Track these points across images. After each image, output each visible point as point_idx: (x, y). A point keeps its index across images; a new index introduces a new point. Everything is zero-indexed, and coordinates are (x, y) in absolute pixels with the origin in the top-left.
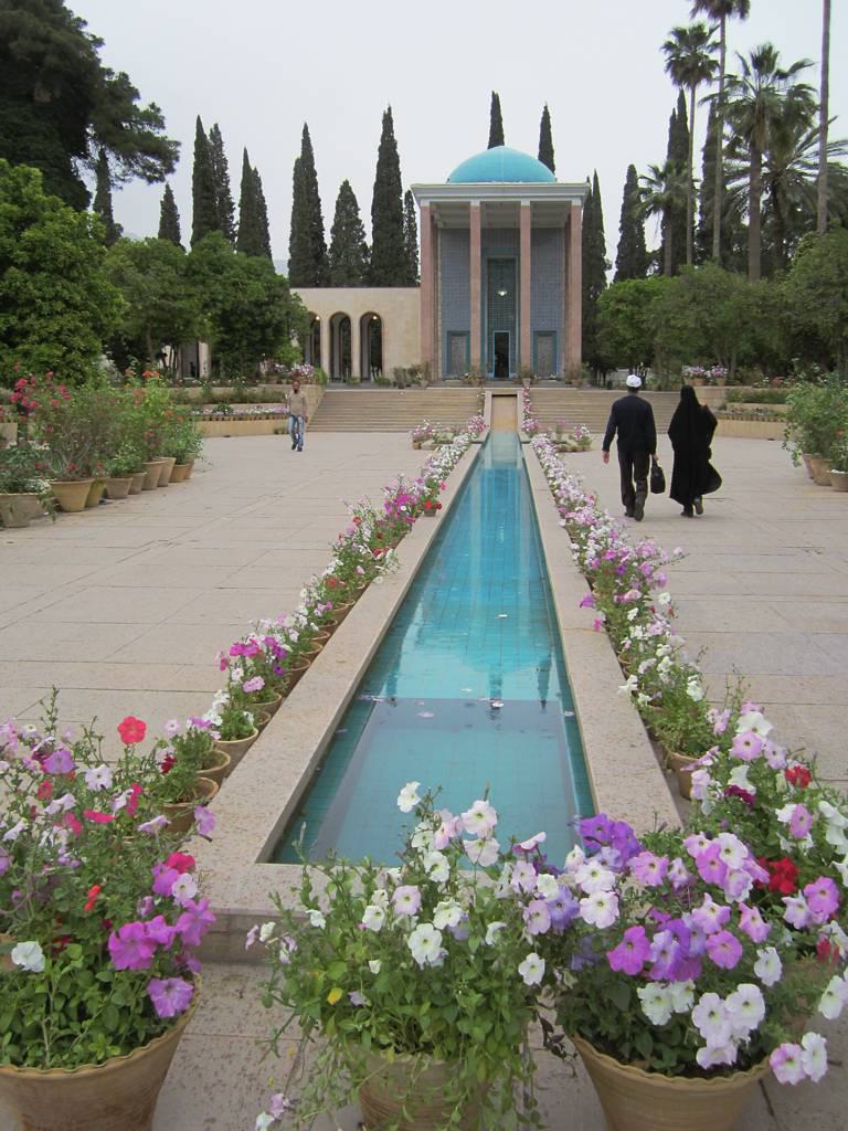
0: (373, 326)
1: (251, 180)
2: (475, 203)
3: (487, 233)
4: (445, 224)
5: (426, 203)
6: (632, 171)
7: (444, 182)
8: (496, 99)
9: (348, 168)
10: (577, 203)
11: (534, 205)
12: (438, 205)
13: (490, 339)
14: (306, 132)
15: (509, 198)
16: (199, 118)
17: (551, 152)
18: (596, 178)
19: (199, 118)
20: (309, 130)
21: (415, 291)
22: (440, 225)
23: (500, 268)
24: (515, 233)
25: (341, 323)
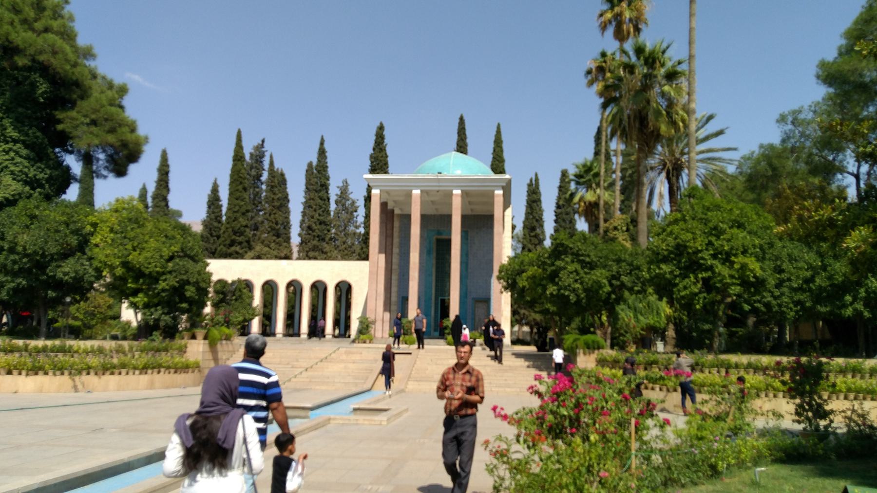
0: (344, 290)
1: (279, 181)
4: (401, 209)
6: (564, 174)
8: (462, 119)
9: (349, 174)
12: (388, 192)
13: (436, 304)
14: (322, 143)
18: (537, 180)
20: (326, 146)
21: (365, 264)
22: (397, 211)
23: (438, 250)
24: (448, 218)
25: (319, 288)
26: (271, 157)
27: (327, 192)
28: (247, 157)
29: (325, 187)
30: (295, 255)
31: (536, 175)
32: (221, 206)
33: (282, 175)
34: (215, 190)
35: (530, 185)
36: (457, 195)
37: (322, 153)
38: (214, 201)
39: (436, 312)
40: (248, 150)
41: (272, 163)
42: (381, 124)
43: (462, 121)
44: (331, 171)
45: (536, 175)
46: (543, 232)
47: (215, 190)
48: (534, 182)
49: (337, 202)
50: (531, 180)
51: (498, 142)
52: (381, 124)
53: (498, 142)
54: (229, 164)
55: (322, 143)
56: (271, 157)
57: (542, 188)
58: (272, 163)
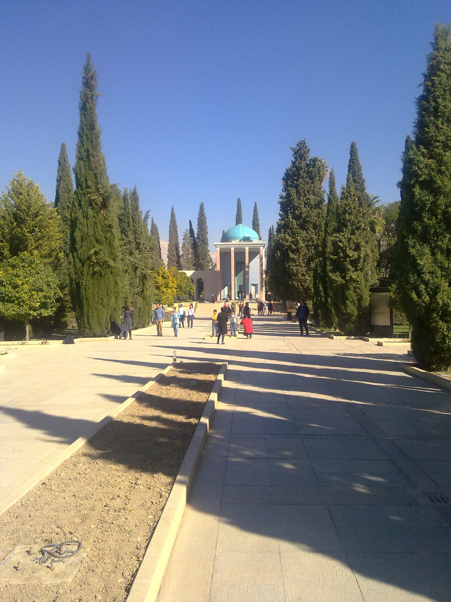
5: (218, 249)
8: (239, 200)
14: (172, 210)
17: (258, 225)
26: (152, 219)
27: (177, 233)
29: (176, 231)
33: (156, 226)
35: (270, 230)
37: (173, 215)
41: (153, 221)
43: (239, 200)
49: (183, 239)
51: (255, 210)
53: (255, 210)
55: (172, 210)
56: (152, 219)
58: (153, 221)
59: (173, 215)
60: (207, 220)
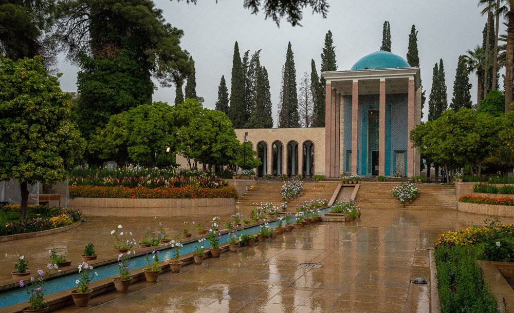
0: (309, 146)
1: (262, 75)
2: (355, 81)
3: (361, 98)
7: (350, 70)
10: (412, 78)
11: (388, 81)
12: (337, 83)
14: (290, 46)
15: (373, 77)
16: (236, 43)
19: (236, 43)
20: (292, 49)
23: (371, 119)
24: (376, 97)
25: (293, 146)
28: (242, 60)
30: (276, 124)
31: (441, 61)
32: (228, 94)
34: (223, 82)
36: (382, 82)
37: (290, 54)
38: (222, 89)
39: (369, 160)
40: (242, 56)
42: (329, 31)
44: (296, 67)
45: (441, 61)
46: (446, 103)
47: (223, 82)
48: (439, 66)
50: (436, 65)
52: (329, 31)
54: (231, 65)
55: (290, 46)
57: (445, 71)
59: (290, 54)
60: (336, 58)
